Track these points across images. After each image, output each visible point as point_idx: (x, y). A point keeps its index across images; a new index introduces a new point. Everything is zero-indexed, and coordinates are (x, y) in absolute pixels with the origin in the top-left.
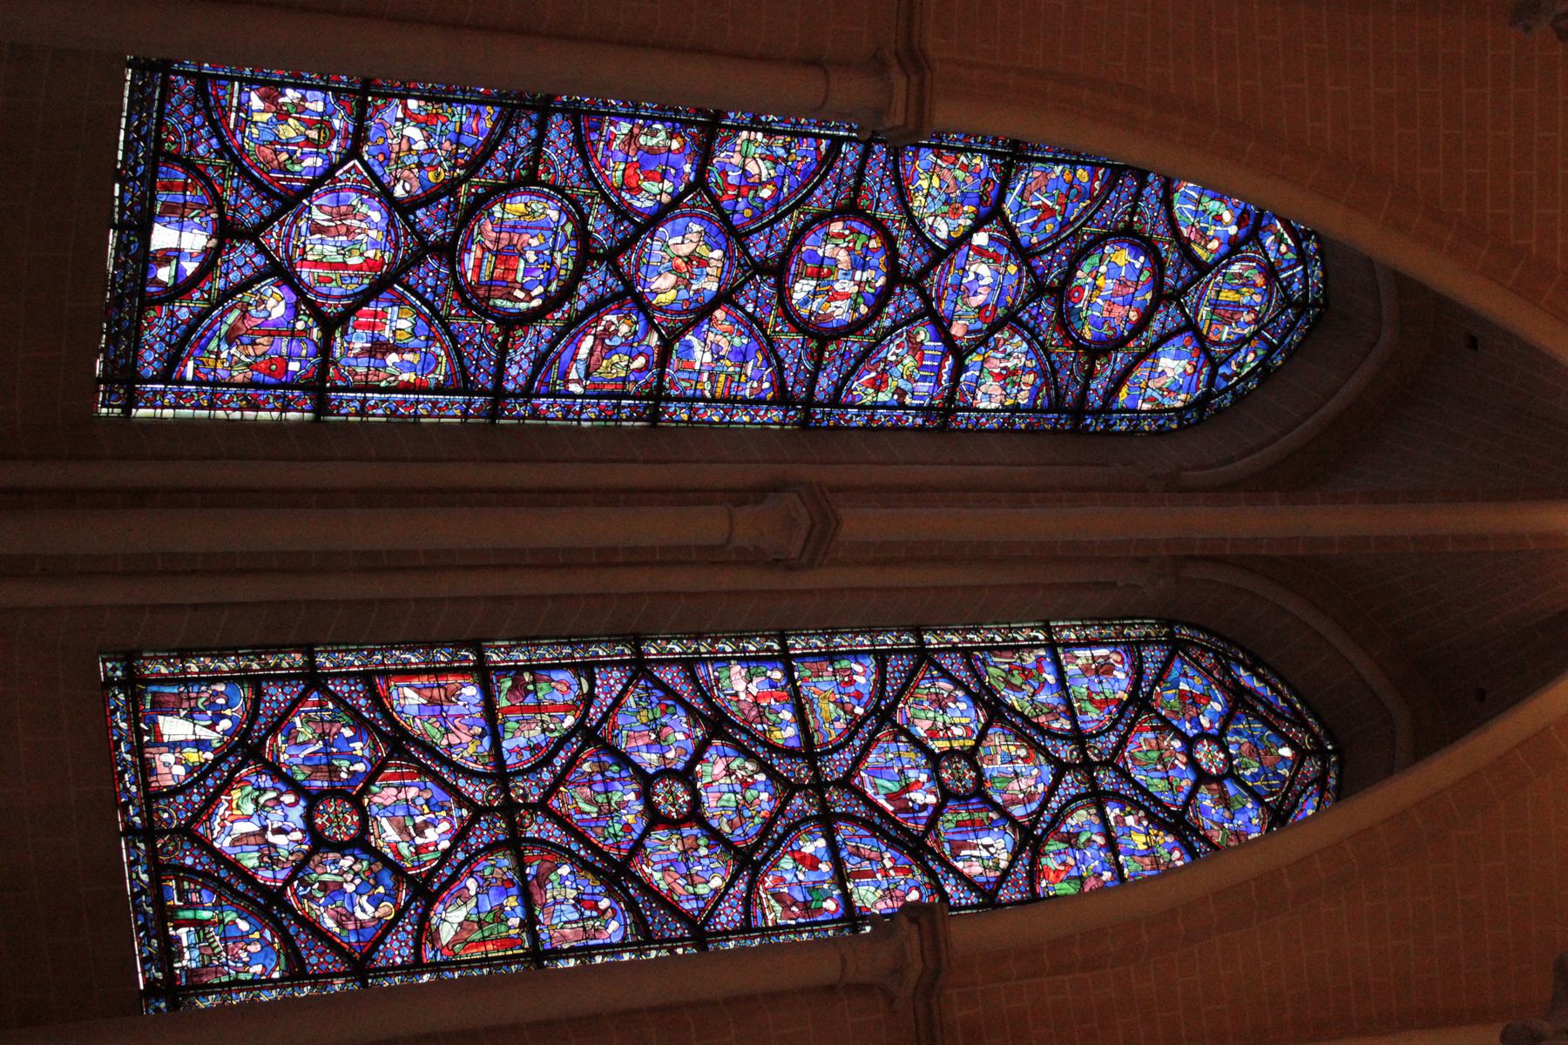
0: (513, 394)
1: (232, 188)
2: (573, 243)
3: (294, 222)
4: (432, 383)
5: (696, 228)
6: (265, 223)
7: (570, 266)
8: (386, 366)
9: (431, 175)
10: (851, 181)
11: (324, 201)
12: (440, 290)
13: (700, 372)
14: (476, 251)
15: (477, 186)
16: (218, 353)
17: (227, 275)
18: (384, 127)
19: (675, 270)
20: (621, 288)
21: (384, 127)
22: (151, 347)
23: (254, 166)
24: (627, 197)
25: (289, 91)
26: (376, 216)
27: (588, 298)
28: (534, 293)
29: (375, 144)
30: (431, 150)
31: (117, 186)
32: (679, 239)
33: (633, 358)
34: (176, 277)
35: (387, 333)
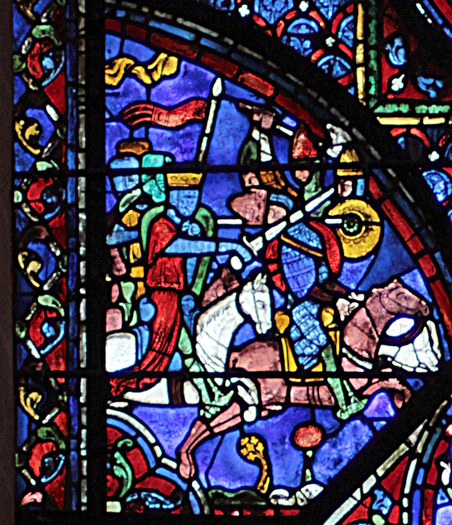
9: (355, 247)
15: (380, 73)
18: (206, 445)
21: (206, 445)
29: (263, 464)
30: (270, 264)
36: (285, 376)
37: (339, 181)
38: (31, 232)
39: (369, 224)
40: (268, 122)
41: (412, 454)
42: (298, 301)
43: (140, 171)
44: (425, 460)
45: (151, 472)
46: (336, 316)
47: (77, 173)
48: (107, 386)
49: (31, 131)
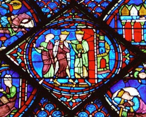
3: (58, 88)
9: (16, 8)
26: (49, 37)
39: (19, 4)
41: (27, 42)
44: (30, 43)
46: (11, 19)
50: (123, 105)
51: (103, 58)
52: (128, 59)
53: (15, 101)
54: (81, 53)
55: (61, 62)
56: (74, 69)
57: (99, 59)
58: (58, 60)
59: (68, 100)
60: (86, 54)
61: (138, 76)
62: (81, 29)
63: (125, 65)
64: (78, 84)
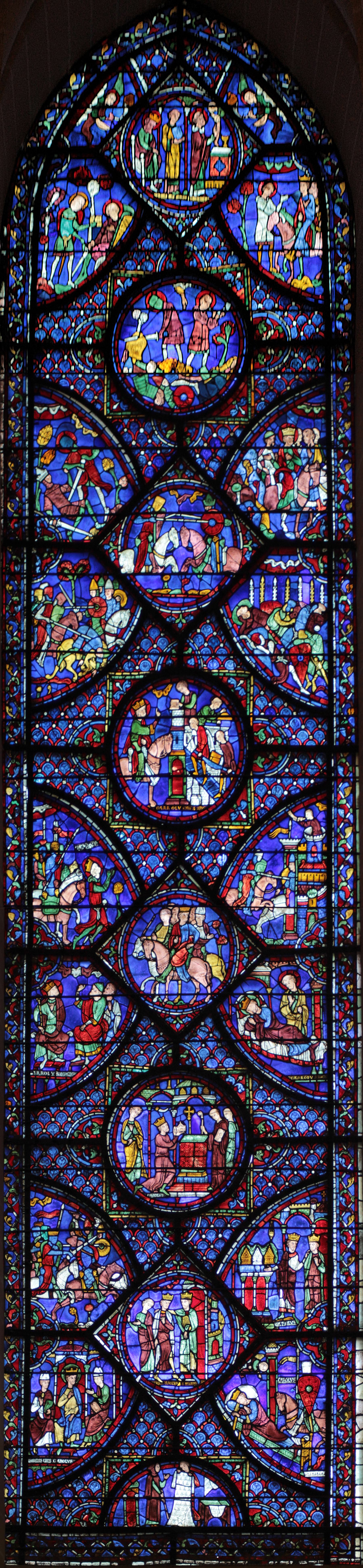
0: (329, 1124)
1: (130, 1454)
2: (163, 1085)
3: (159, 1387)
4: (320, 1215)
5: (138, 947)
6: (163, 1417)
7: (187, 1083)
8: (303, 1269)
9: (103, 1253)
10: (75, 761)
11: (136, 1361)
12: (220, 1224)
13: (298, 907)
14: (178, 1192)
15: (110, 1202)
16: (296, 1447)
17: (215, 1449)
18: (60, 1309)
19: (185, 963)
20: (209, 1020)
21: (60, 1309)
22: (292, 1515)
23: (107, 1434)
24: (111, 1034)
25: (34, 1409)
26: (148, 1305)
27: (220, 1057)
28: (217, 1117)
29: (76, 1316)
30: (78, 1258)
31: (134, 1564)
32: (152, 964)
33: (285, 990)
34: (219, 1499)
35: (268, 1274)
36: (82, 1290)
37: (98, 1234)
38: (9, 1249)
39: (106, 1246)
40: (77, 1217)
41: (119, 1313)
42: (86, 1269)
43: (40, 1231)
45: (44, 1318)
47: (22, 1232)
48: (31, 1293)
49: (9, 1219)
50: (238, 1412)
51: (216, 1340)
52: (247, 1339)
53: (108, 1408)
54: (189, 1332)
55: (164, 1347)
56: (179, 1357)
57: (211, 1340)
58: (159, 1344)
59: (172, 1406)
60: (194, 1334)
61: (258, 1367)
62: (188, 1291)
63: (242, 1351)
64: (183, 1381)
